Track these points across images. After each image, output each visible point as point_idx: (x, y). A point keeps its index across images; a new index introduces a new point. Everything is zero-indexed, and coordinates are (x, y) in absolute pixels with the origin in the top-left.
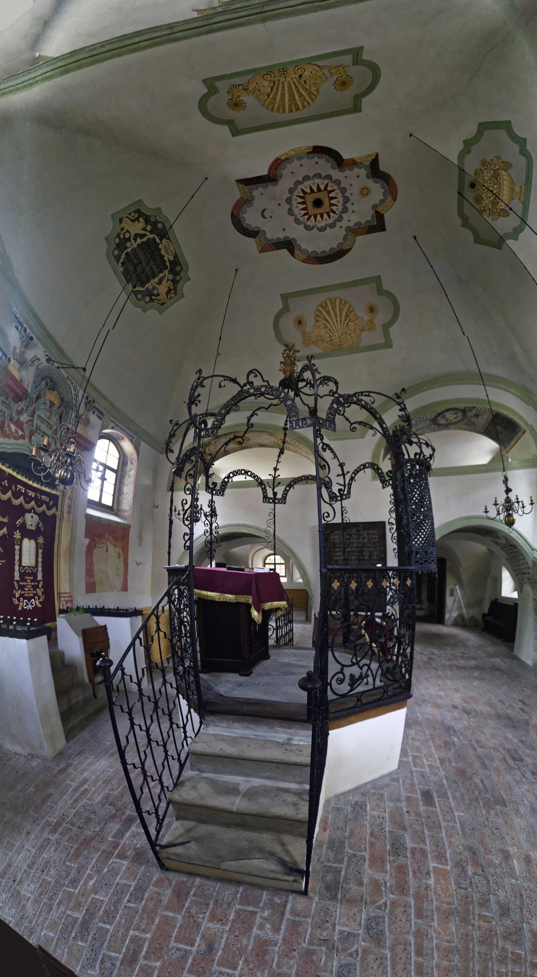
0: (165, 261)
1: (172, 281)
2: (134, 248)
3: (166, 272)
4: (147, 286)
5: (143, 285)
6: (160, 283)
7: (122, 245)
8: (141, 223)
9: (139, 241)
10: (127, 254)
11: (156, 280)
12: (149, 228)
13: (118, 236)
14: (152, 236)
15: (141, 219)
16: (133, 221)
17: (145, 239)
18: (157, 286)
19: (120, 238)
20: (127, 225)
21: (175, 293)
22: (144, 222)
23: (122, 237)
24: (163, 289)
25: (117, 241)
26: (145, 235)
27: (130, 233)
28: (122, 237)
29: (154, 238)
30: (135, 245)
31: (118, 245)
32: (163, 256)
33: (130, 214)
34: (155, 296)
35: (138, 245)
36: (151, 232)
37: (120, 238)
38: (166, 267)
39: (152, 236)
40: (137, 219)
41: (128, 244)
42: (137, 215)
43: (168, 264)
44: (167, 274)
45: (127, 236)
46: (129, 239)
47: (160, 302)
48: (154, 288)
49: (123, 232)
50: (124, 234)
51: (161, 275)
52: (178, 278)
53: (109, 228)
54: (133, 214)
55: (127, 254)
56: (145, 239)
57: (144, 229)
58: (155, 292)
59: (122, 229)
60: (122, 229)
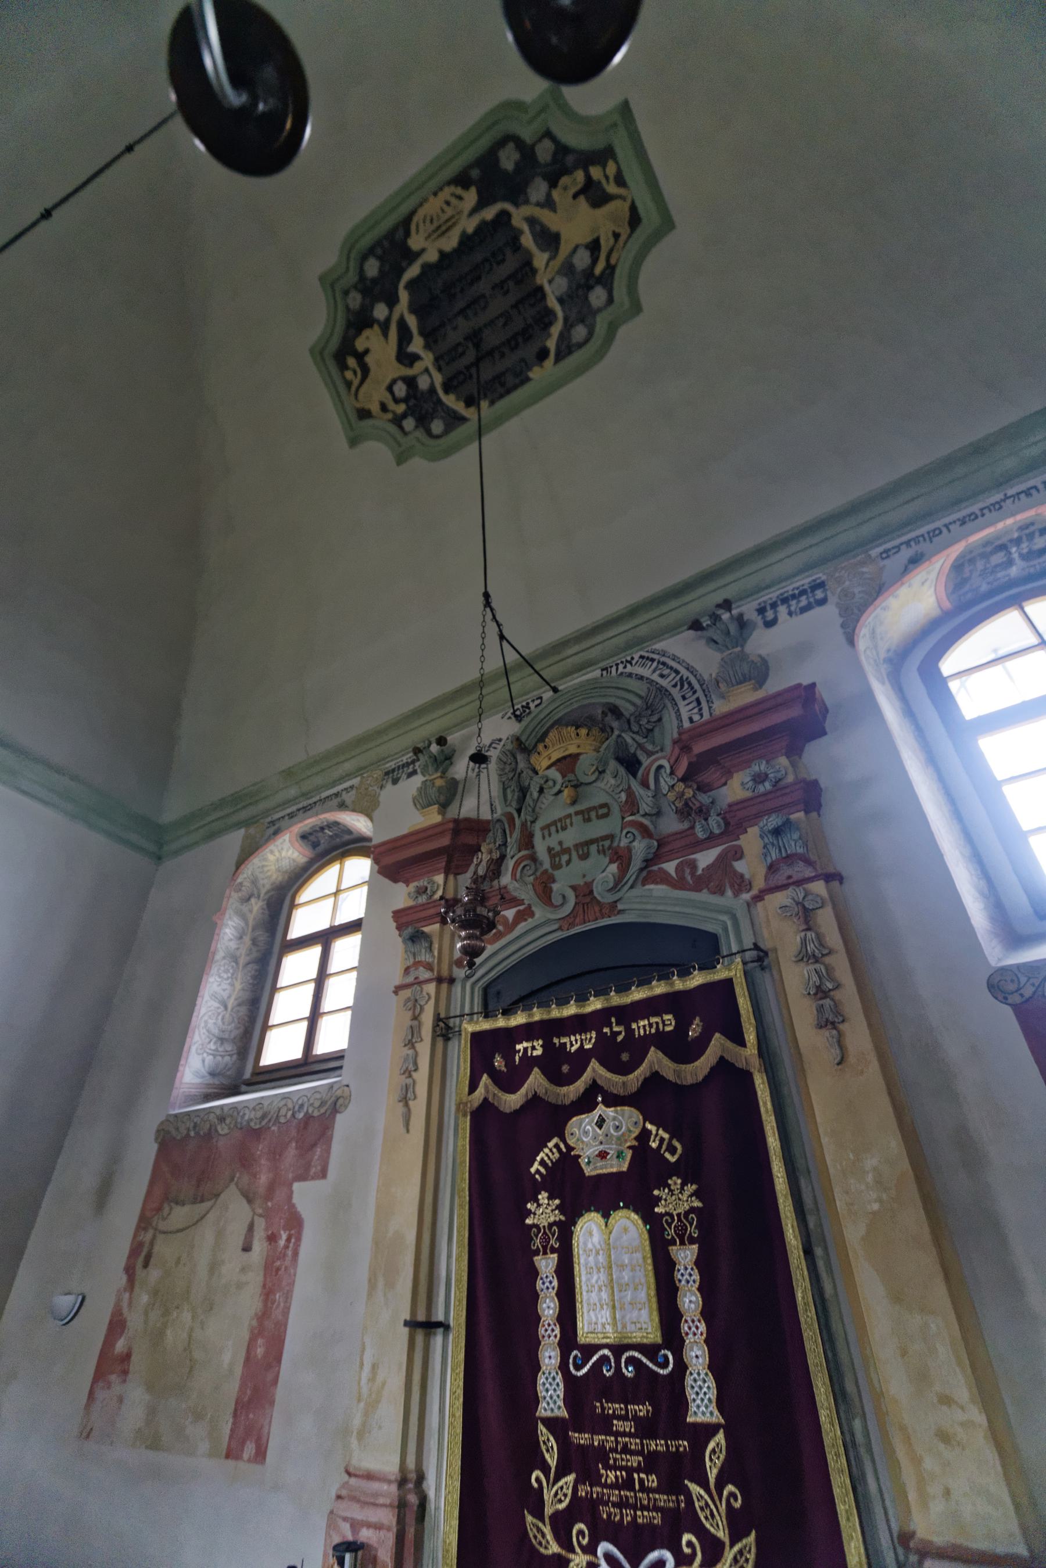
0: (482, 227)
1: (553, 184)
2: (437, 360)
3: (518, 216)
4: (552, 302)
5: (546, 318)
6: (550, 240)
7: (420, 407)
8: (369, 340)
9: (417, 345)
10: (447, 388)
11: (540, 259)
12: (380, 311)
13: (398, 421)
14: (404, 296)
15: (360, 344)
16: (365, 371)
17: (412, 321)
18: (564, 250)
19: (404, 416)
20: (373, 395)
21: (604, 155)
22: (367, 332)
23: (401, 408)
24: (576, 223)
25: (409, 423)
26: (402, 325)
27: (394, 382)
28: (401, 408)
29: (411, 285)
30: (428, 359)
31: (423, 421)
32: (467, 242)
33: (349, 384)
34: (595, 261)
35: (427, 346)
36: (392, 302)
37: (404, 416)
38: (504, 217)
39: (404, 296)
40: (360, 357)
41: (423, 383)
42: (351, 362)
43: (489, 213)
44: (526, 210)
45: (401, 390)
46: (411, 382)
47: (625, 231)
48: (568, 269)
49: (391, 405)
50: (397, 401)
51: (527, 240)
52: (544, 152)
53: (377, 451)
54: (349, 375)
55: (447, 388)
56: (412, 321)
57: (385, 327)
58: (582, 259)
59: (384, 408)
60: (384, 408)
